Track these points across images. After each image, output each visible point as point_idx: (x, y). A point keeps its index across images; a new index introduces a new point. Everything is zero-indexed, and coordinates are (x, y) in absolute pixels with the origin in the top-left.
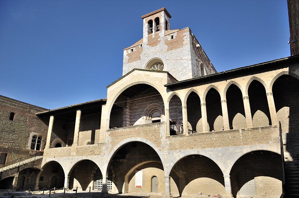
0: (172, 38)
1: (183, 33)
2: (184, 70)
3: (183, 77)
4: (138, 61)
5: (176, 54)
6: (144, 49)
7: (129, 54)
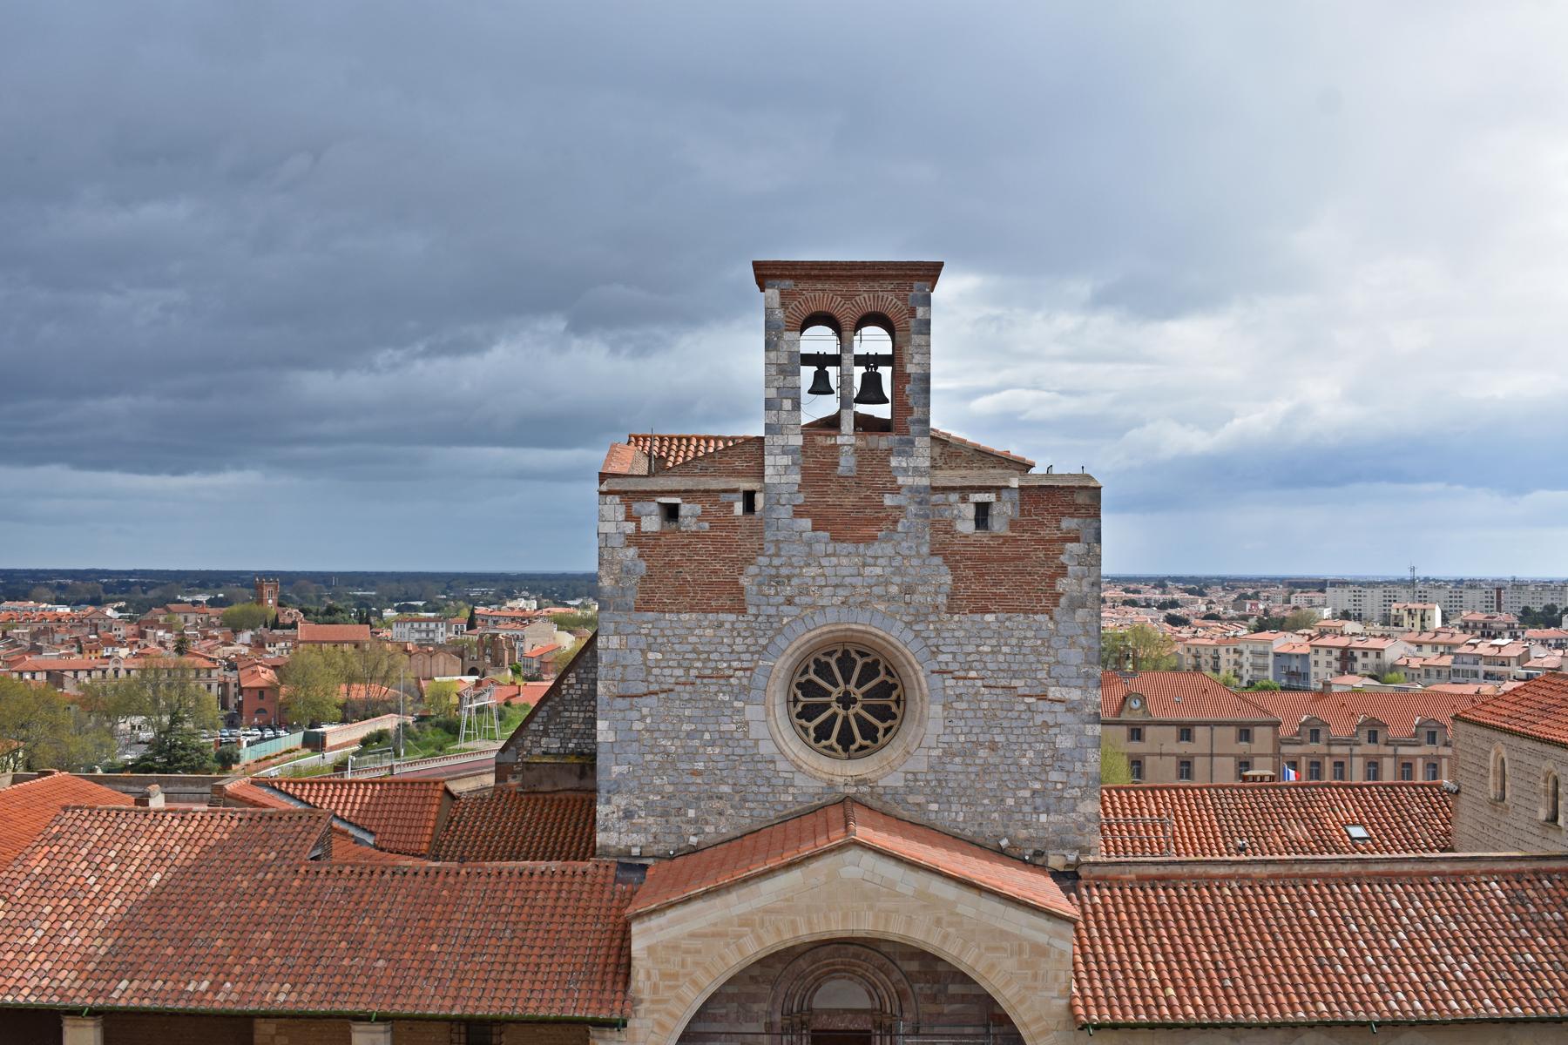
0: (983, 511)
1: (1063, 515)
2: (1054, 776)
3: (1043, 818)
4: (722, 616)
5: (1005, 649)
6: (768, 535)
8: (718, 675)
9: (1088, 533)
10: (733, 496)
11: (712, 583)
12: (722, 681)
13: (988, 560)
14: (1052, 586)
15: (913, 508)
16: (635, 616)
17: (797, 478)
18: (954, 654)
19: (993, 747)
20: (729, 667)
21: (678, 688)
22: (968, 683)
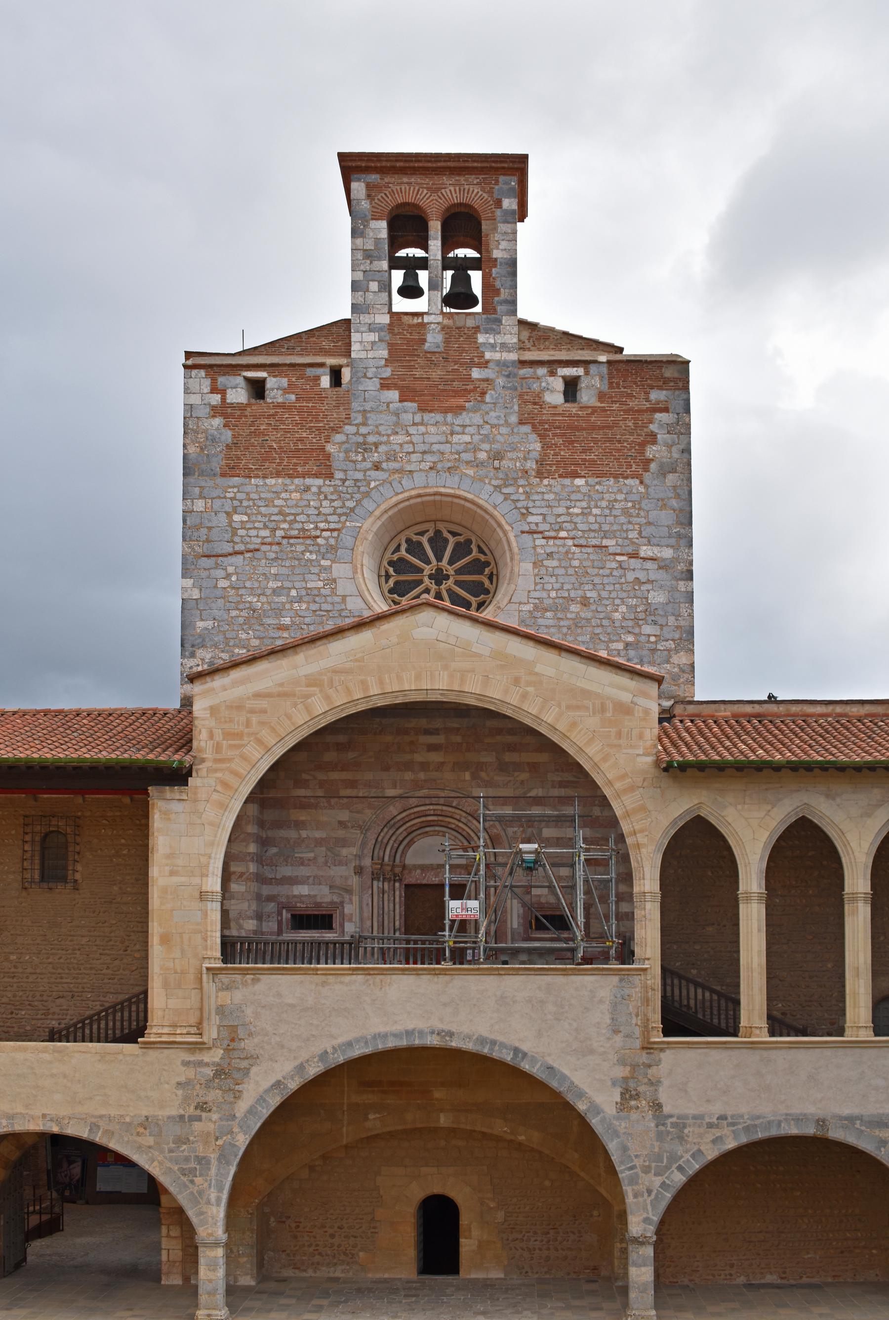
0: (571, 387)
1: (652, 387)
2: (647, 629)
4: (309, 481)
5: (595, 511)
6: (355, 405)
7: (232, 406)
8: (304, 535)
9: (678, 404)
10: (319, 371)
11: (298, 450)
12: (309, 542)
13: (578, 429)
14: (642, 452)
15: (501, 381)
16: (220, 481)
17: (385, 353)
18: (544, 515)
19: (585, 602)
20: (316, 528)
21: (264, 548)
22: (558, 542)
